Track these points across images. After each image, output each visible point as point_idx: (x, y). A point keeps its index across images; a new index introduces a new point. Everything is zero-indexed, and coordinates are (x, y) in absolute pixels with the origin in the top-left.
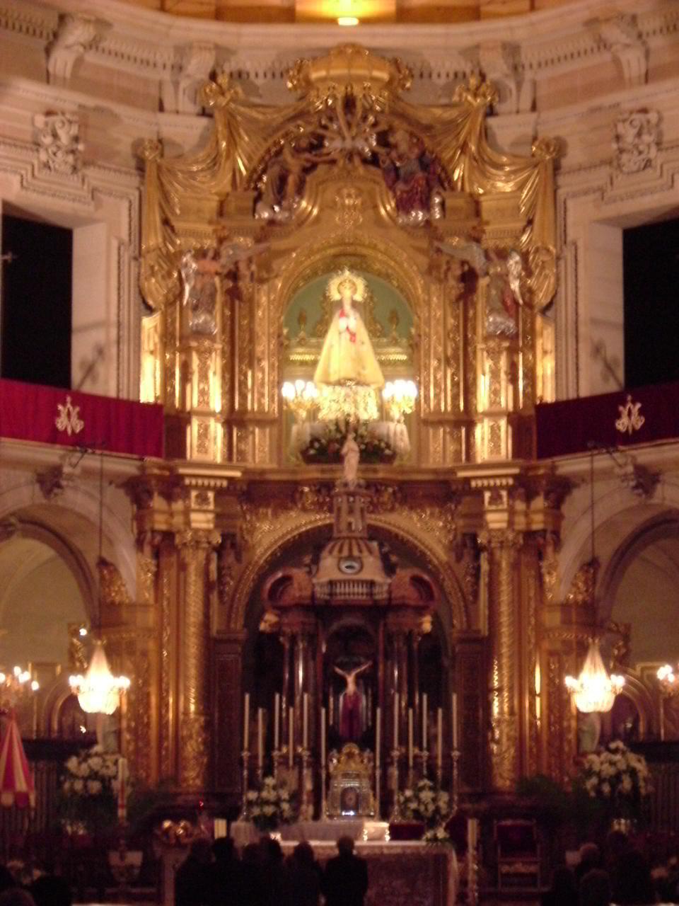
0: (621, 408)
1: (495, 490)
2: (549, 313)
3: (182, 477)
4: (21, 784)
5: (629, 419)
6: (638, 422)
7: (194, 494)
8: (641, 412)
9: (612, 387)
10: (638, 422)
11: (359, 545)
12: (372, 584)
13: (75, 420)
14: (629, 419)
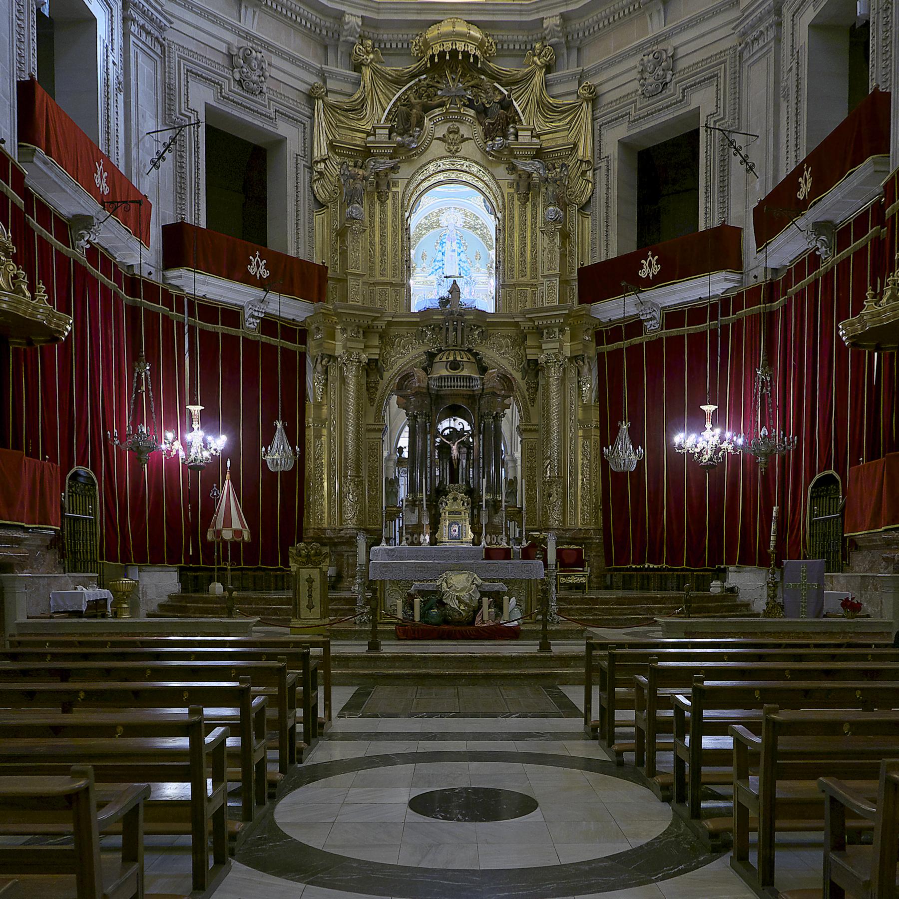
0: (643, 261)
4: (236, 524)
6: (656, 269)
8: (658, 263)
9: (632, 248)
11: (460, 354)
12: (470, 378)
13: (262, 270)
14: (649, 268)
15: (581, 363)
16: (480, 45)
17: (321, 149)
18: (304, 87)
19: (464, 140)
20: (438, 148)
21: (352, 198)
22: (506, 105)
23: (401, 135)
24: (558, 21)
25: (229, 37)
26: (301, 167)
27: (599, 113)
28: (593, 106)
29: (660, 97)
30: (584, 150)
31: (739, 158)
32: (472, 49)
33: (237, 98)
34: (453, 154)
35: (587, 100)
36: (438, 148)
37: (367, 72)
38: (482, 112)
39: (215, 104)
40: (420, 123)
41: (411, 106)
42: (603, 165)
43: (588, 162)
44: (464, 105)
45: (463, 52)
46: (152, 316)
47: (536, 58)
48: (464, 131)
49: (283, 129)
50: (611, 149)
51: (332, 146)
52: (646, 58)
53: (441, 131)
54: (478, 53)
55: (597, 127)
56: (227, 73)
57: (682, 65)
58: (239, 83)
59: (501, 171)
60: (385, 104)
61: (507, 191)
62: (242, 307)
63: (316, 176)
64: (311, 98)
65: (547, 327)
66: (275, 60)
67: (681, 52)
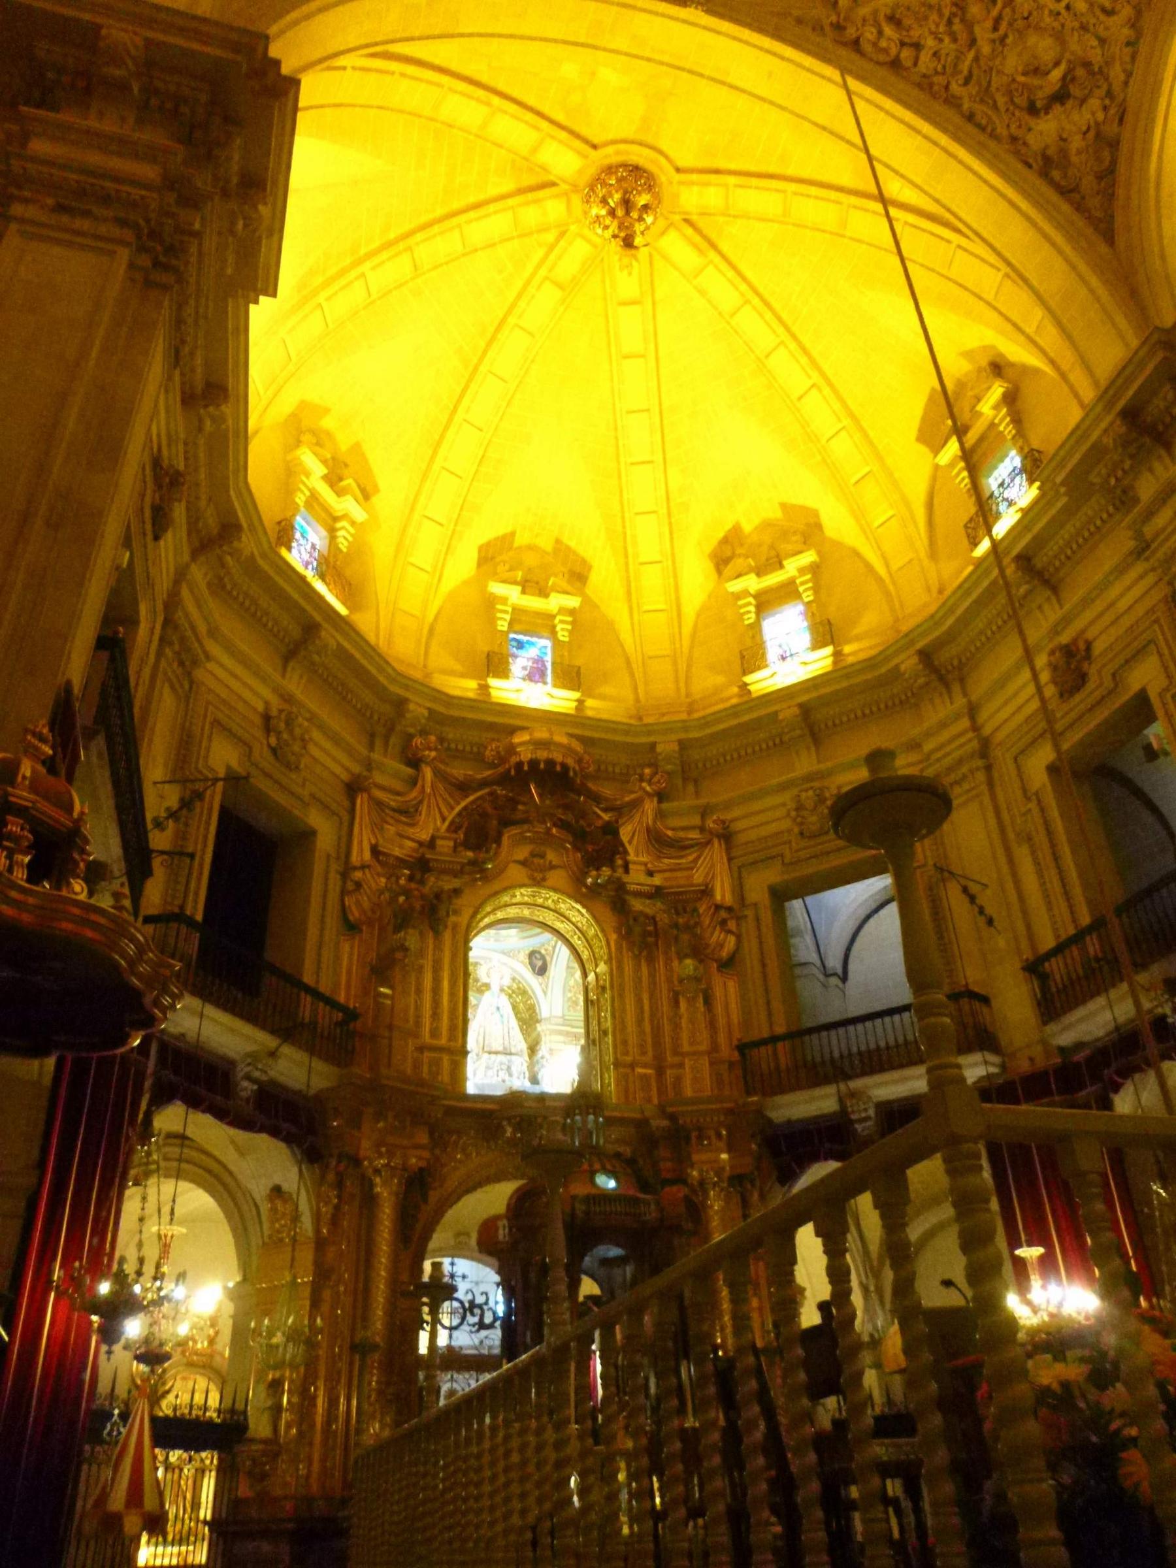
15: (749, 1186)
16: (580, 761)
17: (361, 853)
18: (345, 776)
19: (552, 867)
20: (516, 872)
21: (403, 920)
22: (611, 830)
25: (266, 693)
27: (734, 853)
35: (719, 836)
40: (498, 841)
43: (729, 909)
47: (644, 784)
49: (315, 819)
51: (375, 851)
52: (804, 795)
53: (522, 853)
54: (577, 768)
56: (259, 734)
58: (274, 751)
60: (446, 813)
62: (232, 1063)
63: (350, 886)
64: (353, 788)
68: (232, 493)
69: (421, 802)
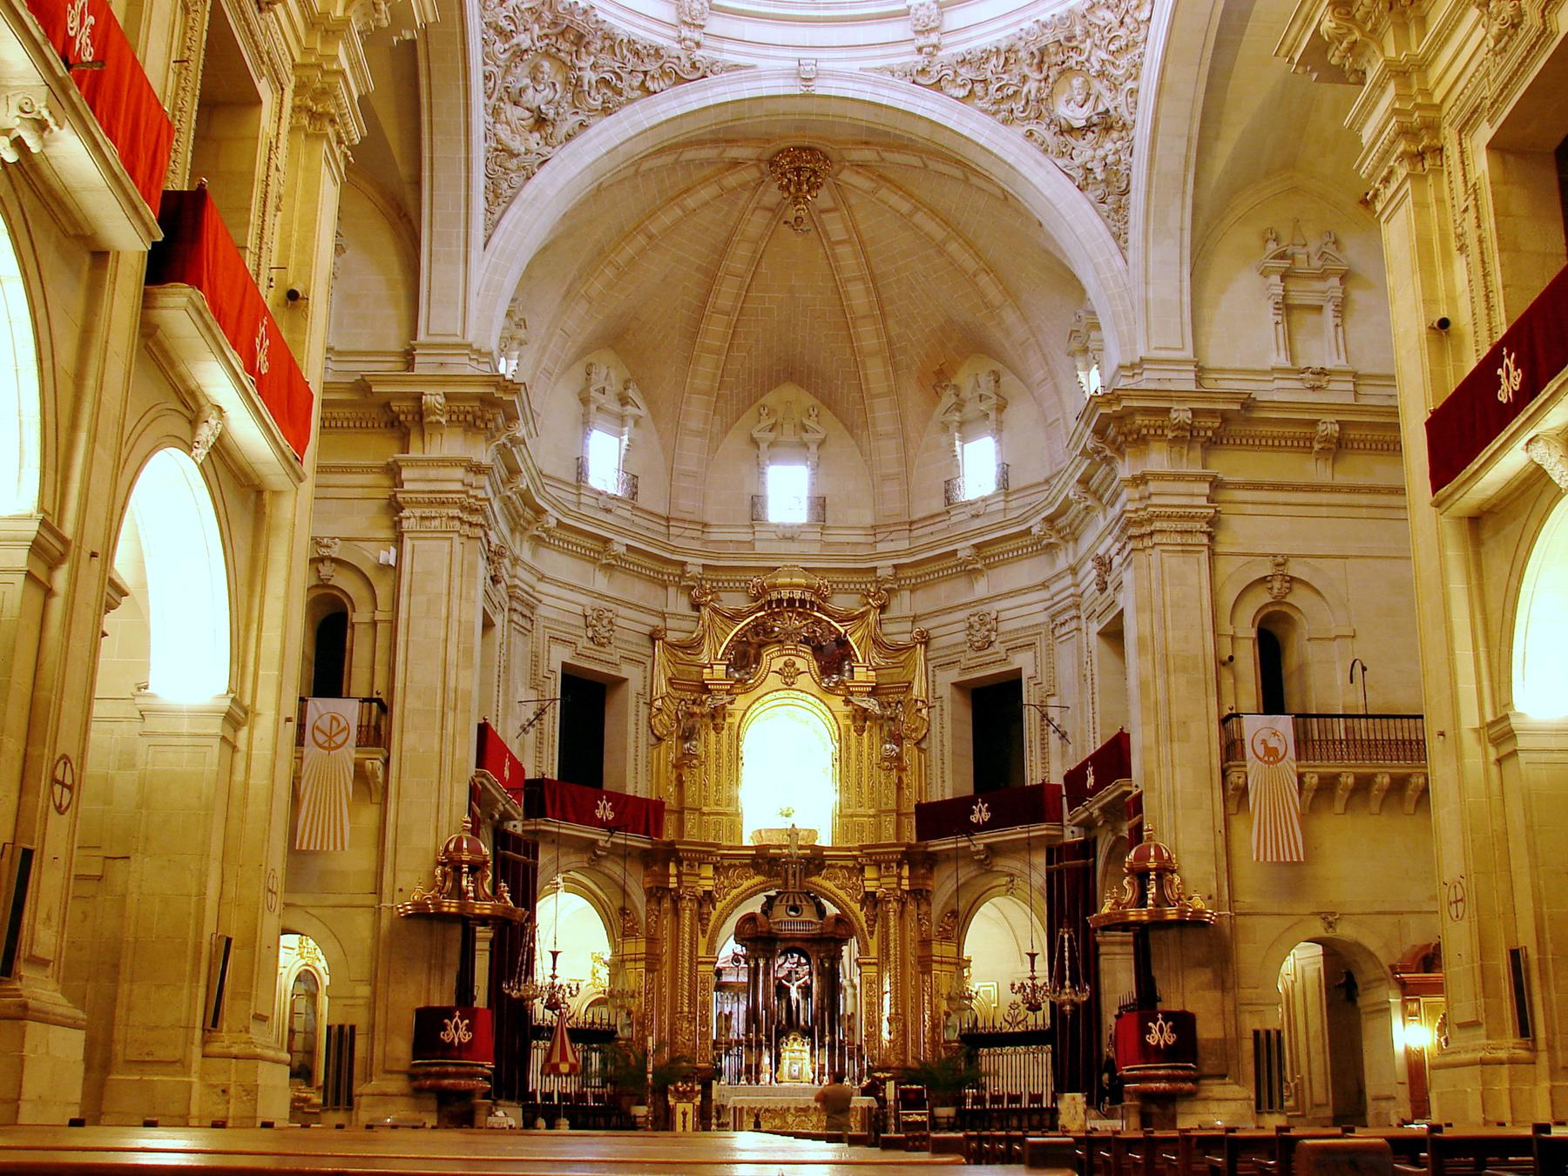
1: (888, 862)
2: (923, 746)
3: (678, 850)
5: (980, 814)
6: (986, 816)
7: (685, 863)
10: (986, 816)
14: (980, 814)
17: (662, 686)
18: (647, 630)
20: (774, 680)
22: (842, 643)
23: (738, 671)
24: (891, 571)
26: (641, 704)
27: (931, 655)
28: (926, 647)
29: (986, 652)
30: (918, 690)
31: (1052, 728)
32: (807, 596)
33: (588, 653)
34: (789, 686)
35: (921, 643)
36: (774, 680)
37: (705, 612)
38: (818, 651)
39: (570, 661)
40: (758, 659)
41: (749, 643)
42: (938, 704)
44: (801, 642)
45: (800, 600)
46: (516, 863)
48: (801, 664)
49: (626, 671)
50: (945, 690)
52: (972, 619)
53: (778, 664)
55: (930, 668)
56: (581, 632)
57: (1003, 627)
58: (592, 639)
59: (837, 702)
61: (843, 722)
65: (884, 861)
66: (622, 611)
67: (1003, 616)
68: (538, 500)
69: (703, 636)
